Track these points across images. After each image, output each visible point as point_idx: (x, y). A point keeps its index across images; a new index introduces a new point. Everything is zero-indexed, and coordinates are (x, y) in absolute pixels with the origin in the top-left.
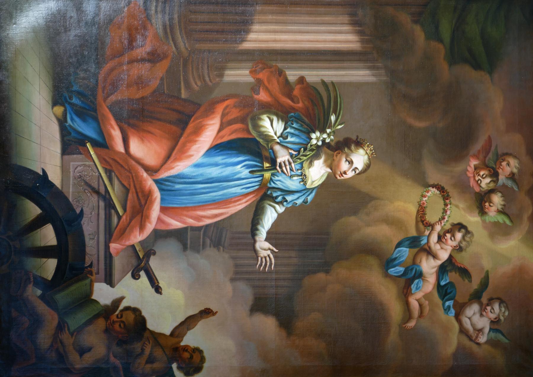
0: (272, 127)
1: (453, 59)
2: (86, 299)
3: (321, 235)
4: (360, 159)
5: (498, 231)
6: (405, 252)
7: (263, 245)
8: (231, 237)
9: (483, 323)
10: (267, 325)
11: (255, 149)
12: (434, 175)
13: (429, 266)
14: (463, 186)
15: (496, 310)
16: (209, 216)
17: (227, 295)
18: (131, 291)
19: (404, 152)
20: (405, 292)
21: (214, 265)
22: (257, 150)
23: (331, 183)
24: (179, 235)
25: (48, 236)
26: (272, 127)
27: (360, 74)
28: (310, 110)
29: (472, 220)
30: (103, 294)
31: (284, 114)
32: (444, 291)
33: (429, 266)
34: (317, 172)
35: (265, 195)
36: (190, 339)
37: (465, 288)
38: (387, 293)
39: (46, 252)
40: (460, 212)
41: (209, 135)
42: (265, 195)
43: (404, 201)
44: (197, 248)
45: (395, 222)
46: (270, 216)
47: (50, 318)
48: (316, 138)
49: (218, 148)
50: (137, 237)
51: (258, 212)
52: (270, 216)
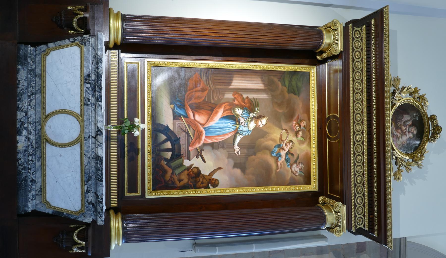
0: (239, 111)
1: (289, 92)
2: (181, 165)
3: (253, 145)
4: (264, 121)
5: (301, 142)
6: (277, 149)
7: (236, 148)
8: (227, 145)
9: (297, 169)
10: (238, 172)
11: (234, 118)
12: (284, 126)
13: (283, 153)
15: (301, 166)
16: (220, 139)
17: (226, 163)
18: (196, 162)
19: (276, 119)
20: (277, 161)
21: (222, 153)
22: (234, 118)
23: (256, 128)
24: (212, 145)
25: (169, 145)
26: (239, 111)
27: (264, 96)
28: (250, 107)
29: (294, 139)
30: (187, 163)
31: (242, 108)
32: (287, 160)
33: (283, 153)
34: (252, 125)
35: (237, 132)
36: (215, 177)
37: (293, 159)
38: (272, 161)
39: (168, 150)
40: (291, 137)
41: (220, 113)
42: (237, 132)
43: (276, 134)
44: (217, 149)
45: (274, 140)
46: (239, 139)
47: (170, 172)
48: (252, 115)
49: (223, 118)
50: (198, 145)
51: (235, 137)
52: (239, 139)
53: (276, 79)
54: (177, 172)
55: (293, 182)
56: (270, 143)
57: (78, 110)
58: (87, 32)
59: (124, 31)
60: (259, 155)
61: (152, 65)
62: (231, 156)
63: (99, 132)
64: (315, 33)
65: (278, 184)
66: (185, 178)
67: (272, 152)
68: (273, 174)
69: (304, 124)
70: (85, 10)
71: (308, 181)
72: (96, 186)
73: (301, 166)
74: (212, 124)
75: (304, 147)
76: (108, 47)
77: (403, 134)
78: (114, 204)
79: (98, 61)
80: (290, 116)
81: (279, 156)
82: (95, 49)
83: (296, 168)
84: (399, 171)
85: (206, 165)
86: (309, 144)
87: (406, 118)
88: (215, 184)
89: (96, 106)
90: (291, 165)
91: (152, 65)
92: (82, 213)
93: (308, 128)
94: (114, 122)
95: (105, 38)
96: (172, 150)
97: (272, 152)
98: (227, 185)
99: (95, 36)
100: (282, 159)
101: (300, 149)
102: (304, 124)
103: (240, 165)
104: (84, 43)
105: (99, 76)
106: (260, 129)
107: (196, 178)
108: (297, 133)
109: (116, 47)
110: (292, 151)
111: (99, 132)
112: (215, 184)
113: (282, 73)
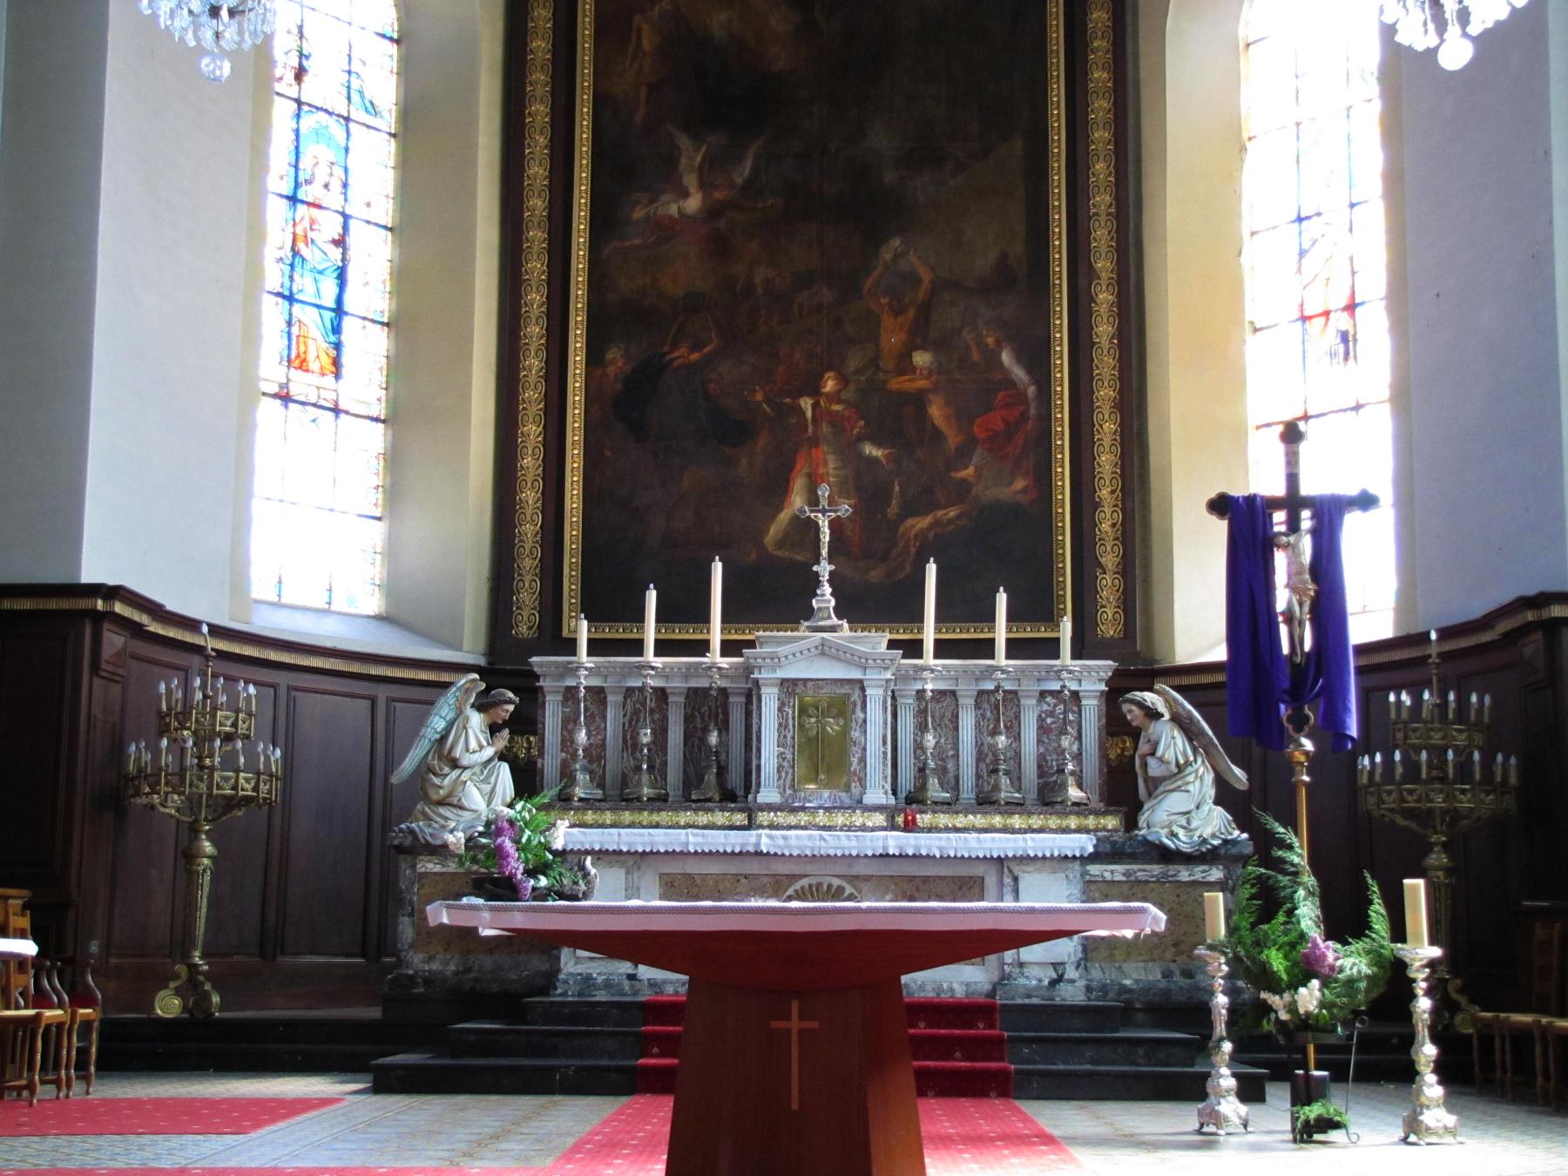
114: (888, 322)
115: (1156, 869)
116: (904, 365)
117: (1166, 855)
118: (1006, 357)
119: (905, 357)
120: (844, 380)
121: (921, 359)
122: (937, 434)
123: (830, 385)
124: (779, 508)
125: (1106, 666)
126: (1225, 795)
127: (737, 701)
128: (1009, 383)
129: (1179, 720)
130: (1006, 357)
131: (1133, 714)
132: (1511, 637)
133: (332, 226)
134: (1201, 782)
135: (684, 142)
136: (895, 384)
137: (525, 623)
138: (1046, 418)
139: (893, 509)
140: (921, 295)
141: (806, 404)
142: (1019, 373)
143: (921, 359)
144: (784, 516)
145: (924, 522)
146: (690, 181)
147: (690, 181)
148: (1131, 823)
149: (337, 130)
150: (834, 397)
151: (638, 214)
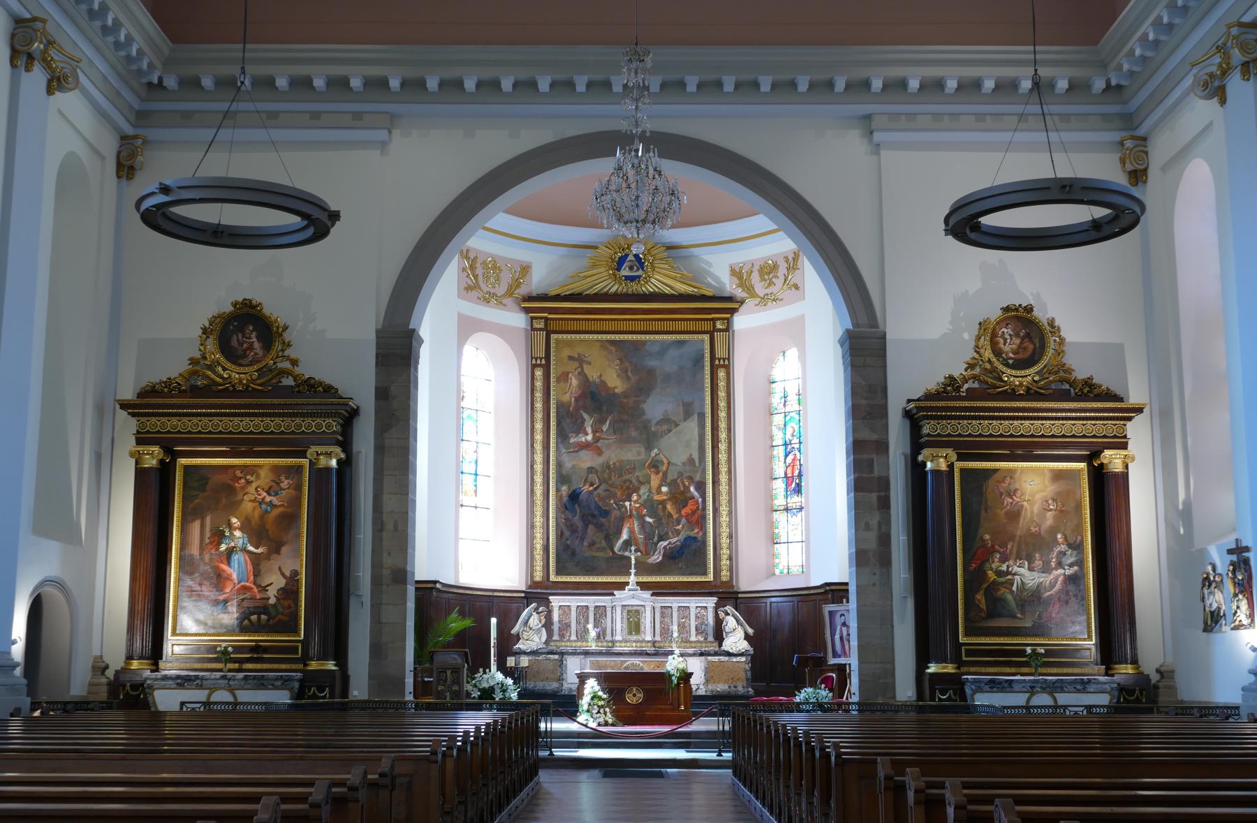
0: (223, 547)
1: (204, 490)
2: (274, 606)
3: (257, 532)
4: (234, 520)
5: (258, 477)
6: (263, 506)
7: (259, 551)
8: (256, 560)
9: (286, 482)
10: (284, 549)
11: (230, 551)
12: (240, 497)
13: (268, 499)
14: (243, 488)
15: (282, 478)
16: (250, 567)
17: (275, 562)
18: (272, 593)
19: (233, 507)
20: (276, 506)
21: (264, 566)
22: (230, 551)
23: (241, 529)
24: (255, 576)
25: (254, 617)
26: (223, 547)
27: (208, 520)
28: (219, 536)
29: (254, 485)
30: (272, 601)
31: (220, 544)
32: (276, 494)
33: (268, 499)
34: (238, 533)
35: (244, 550)
36: (288, 574)
37: (275, 487)
38: (276, 512)
39: (259, 618)
40: (251, 489)
41: (224, 567)
42: (244, 550)
43: (247, 506)
44: (259, 571)
45: (254, 509)
46: (251, 548)
47: (280, 617)
48: (227, 534)
49: (229, 564)
50: (255, 590)
51: (250, 552)
52: (251, 548)
53: (191, 506)
54: (281, 610)
55: (299, 488)
56: (257, 513)
57: (207, 692)
58: (142, 685)
59: (141, 658)
60: (269, 526)
61: (174, 634)
62: (267, 557)
63: (224, 677)
64: (141, 474)
65: (300, 506)
66: (286, 603)
67: (266, 511)
68: (289, 510)
69: (238, 473)
70: (124, 686)
71: (299, 468)
72: (268, 679)
73: (282, 478)
74: (235, 576)
75: (263, 473)
76: (157, 670)
77: (251, 347)
78: (301, 666)
79: (165, 678)
80: (230, 490)
81: (271, 504)
82: (156, 679)
83: (285, 483)
84: (288, 358)
85: (275, 582)
86: (260, 466)
87: (234, 343)
88: (295, 573)
89: (202, 679)
90: (282, 489)
91: (174, 634)
92: (291, 690)
93: (243, 468)
94: (220, 666)
95: (148, 672)
96: (259, 614)
97: (266, 511)
98: (294, 561)
99: (146, 679)
100: (275, 500)
101: (265, 478)
102: (238, 473)
103: (276, 548)
104: (151, 687)
105: (178, 677)
106: (242, 524)
107: (289, 592)
108: (249, 482)
109: (156, 664)
110: (266, 488)
111: (224, 677)
112: (295, 573)
113: (185, 499)
114: (653, 477)
115: (726, 658)
116: (659, 492)
117: (729, 654)
118: (692, 489)
119: (659, 487)
120: (639, 496)
121: (664, 489)
122: (670, 515)
123: (635, 497)
124: (619, 538)
125: (715, 599)
126: (747, 637)
127: (609, 610)
128: (693, 498)
129: (734, 616)
130: (692, 489)
131: (722, 615)
132: (826, 592)
133: (473, 446)
134: (740, 634)
135: (585, 416)
136: (656, 497)
137: (538, 577)
138: (704, 509)
139: (656, 539)
140: (664, 468)
141: (627, 504)
142: (696, 494)
143: (664, 489)
144: (621, 541)
145: (665, 543)
146: (589, 430)
147: (589, 430)
148: (720, 645)
149: (473, 414)
150: (636, 502)
151: (572, 441)
